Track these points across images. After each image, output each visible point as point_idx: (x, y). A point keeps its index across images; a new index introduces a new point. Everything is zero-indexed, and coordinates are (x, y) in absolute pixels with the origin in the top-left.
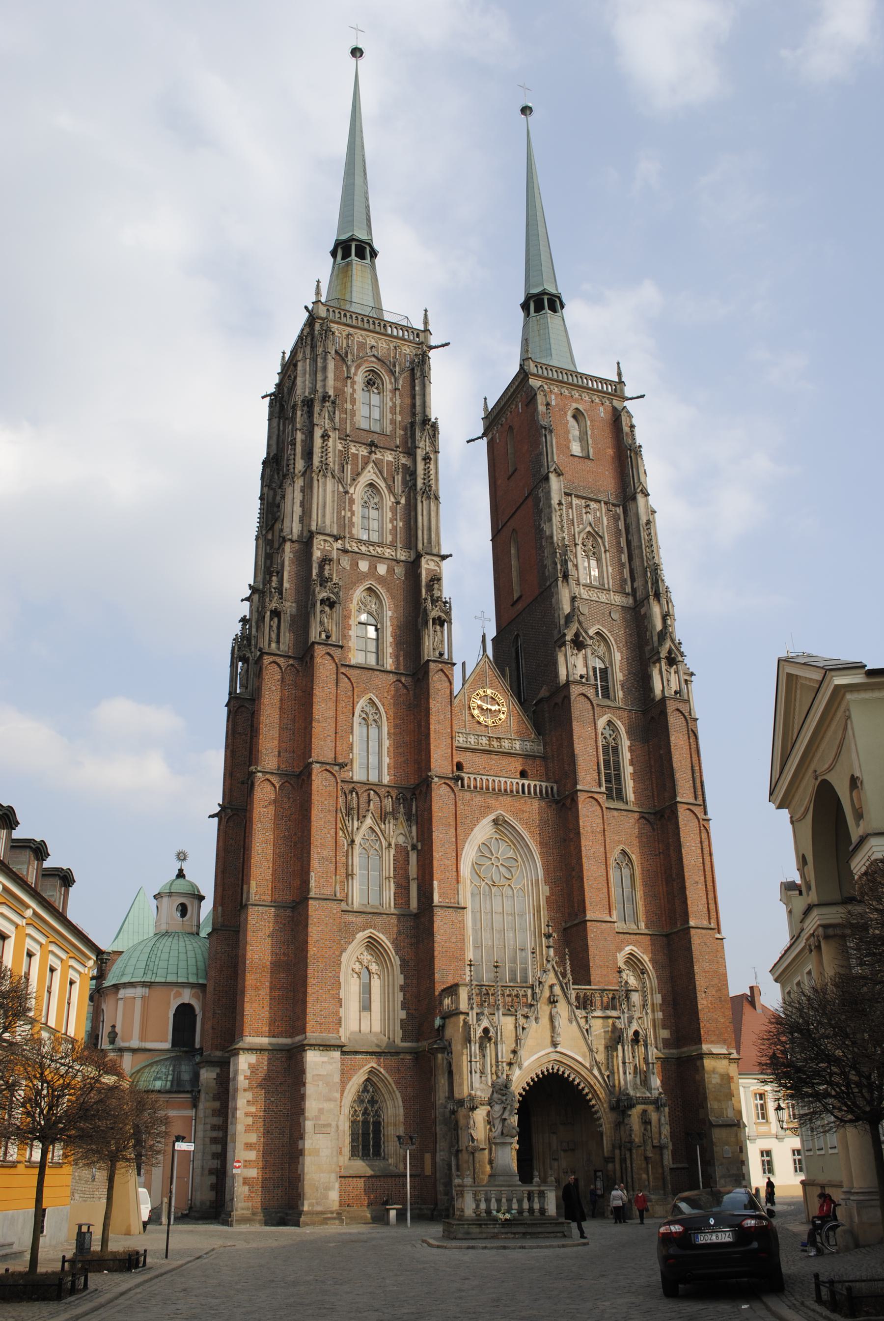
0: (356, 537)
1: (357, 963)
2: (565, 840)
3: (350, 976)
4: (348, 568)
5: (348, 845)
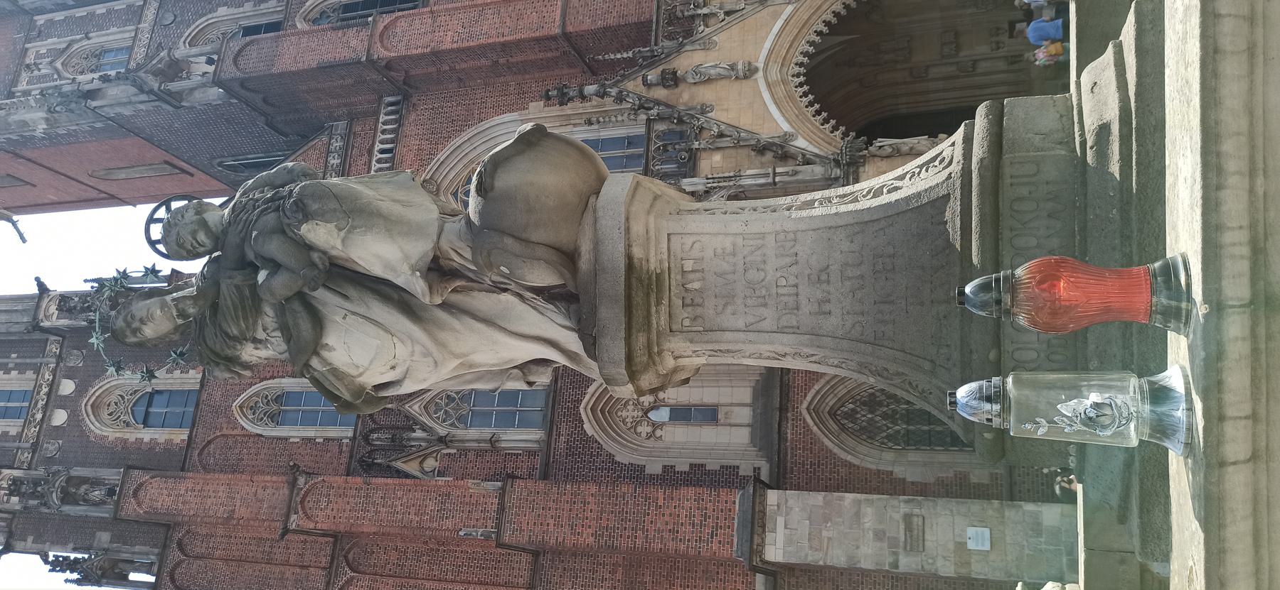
0: (20, 430)
1: (639, 429)
2: (460, 79)
3: (659, 444)
4: (61, 442)
5: (448, 447)
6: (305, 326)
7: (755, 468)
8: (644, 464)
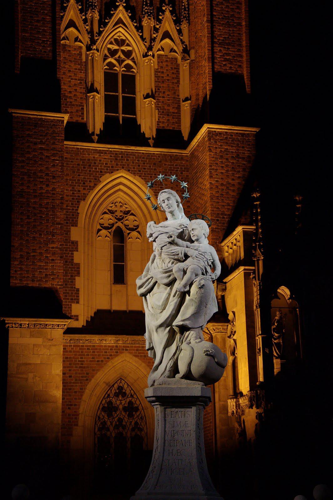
6: (166, 281)
7: (77, 316)
8: (79, 225)
